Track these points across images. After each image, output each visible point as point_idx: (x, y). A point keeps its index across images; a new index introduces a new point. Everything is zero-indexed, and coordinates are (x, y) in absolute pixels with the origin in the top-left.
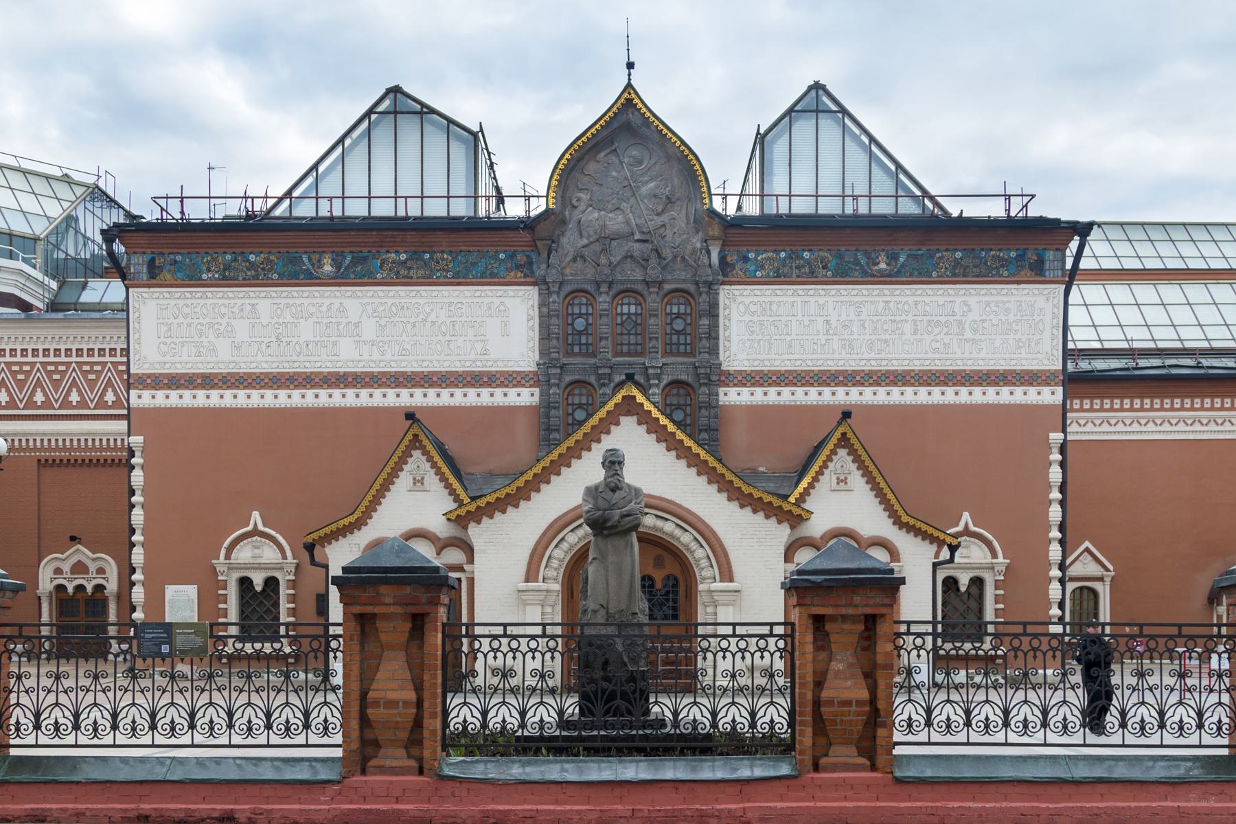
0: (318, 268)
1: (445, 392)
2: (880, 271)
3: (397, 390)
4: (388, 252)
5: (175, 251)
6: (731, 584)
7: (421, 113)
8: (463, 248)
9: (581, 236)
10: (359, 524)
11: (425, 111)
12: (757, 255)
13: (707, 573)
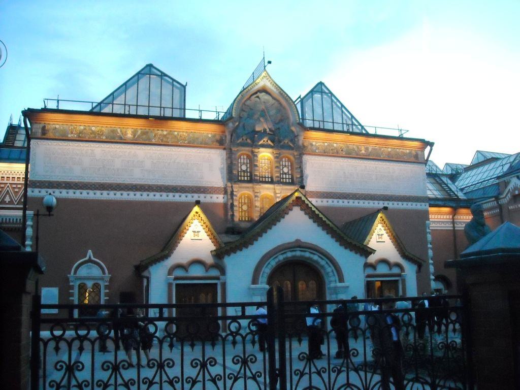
0: (126, 135)
1: (183, 195)
2: (362, 154)
3: (161, 193)
4: (158, 130)
5: (56, 123)
6: (343, 284)
7: (161, 76)
8: (192, 131)
9: (244, 129)
10: (167, 256)
11: (163, 75)
12: (316, 142)
13: (332, 279)
